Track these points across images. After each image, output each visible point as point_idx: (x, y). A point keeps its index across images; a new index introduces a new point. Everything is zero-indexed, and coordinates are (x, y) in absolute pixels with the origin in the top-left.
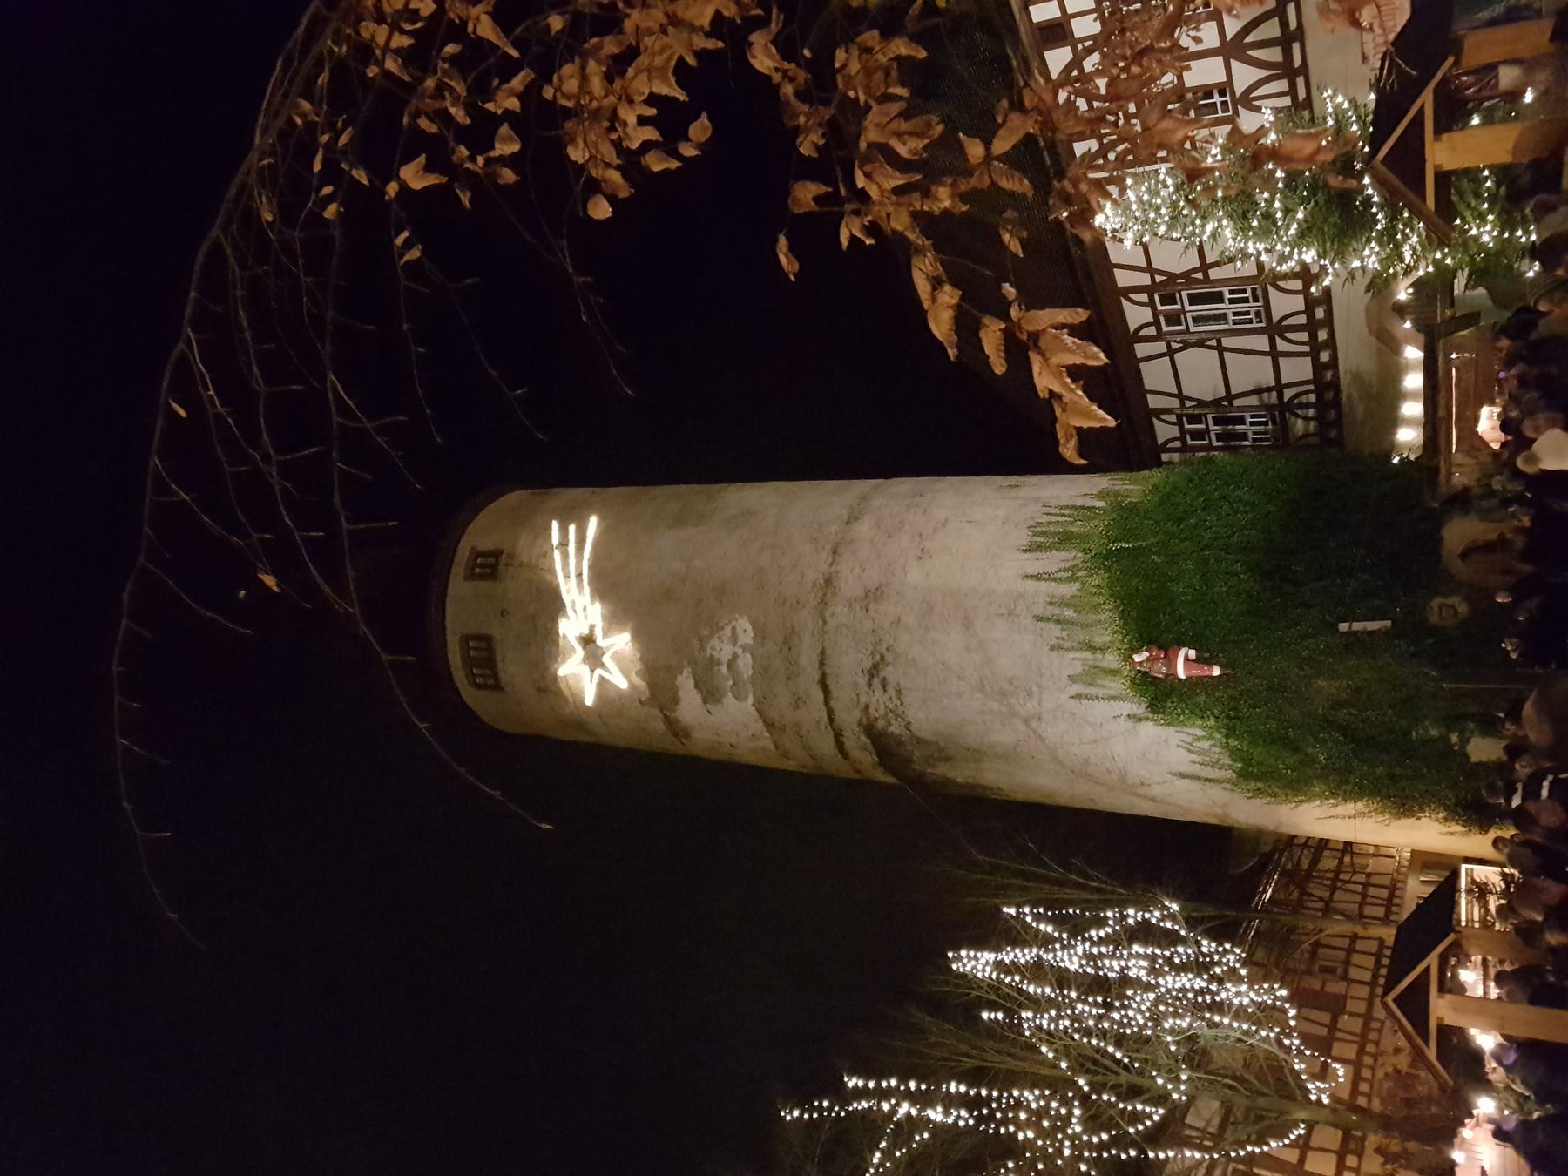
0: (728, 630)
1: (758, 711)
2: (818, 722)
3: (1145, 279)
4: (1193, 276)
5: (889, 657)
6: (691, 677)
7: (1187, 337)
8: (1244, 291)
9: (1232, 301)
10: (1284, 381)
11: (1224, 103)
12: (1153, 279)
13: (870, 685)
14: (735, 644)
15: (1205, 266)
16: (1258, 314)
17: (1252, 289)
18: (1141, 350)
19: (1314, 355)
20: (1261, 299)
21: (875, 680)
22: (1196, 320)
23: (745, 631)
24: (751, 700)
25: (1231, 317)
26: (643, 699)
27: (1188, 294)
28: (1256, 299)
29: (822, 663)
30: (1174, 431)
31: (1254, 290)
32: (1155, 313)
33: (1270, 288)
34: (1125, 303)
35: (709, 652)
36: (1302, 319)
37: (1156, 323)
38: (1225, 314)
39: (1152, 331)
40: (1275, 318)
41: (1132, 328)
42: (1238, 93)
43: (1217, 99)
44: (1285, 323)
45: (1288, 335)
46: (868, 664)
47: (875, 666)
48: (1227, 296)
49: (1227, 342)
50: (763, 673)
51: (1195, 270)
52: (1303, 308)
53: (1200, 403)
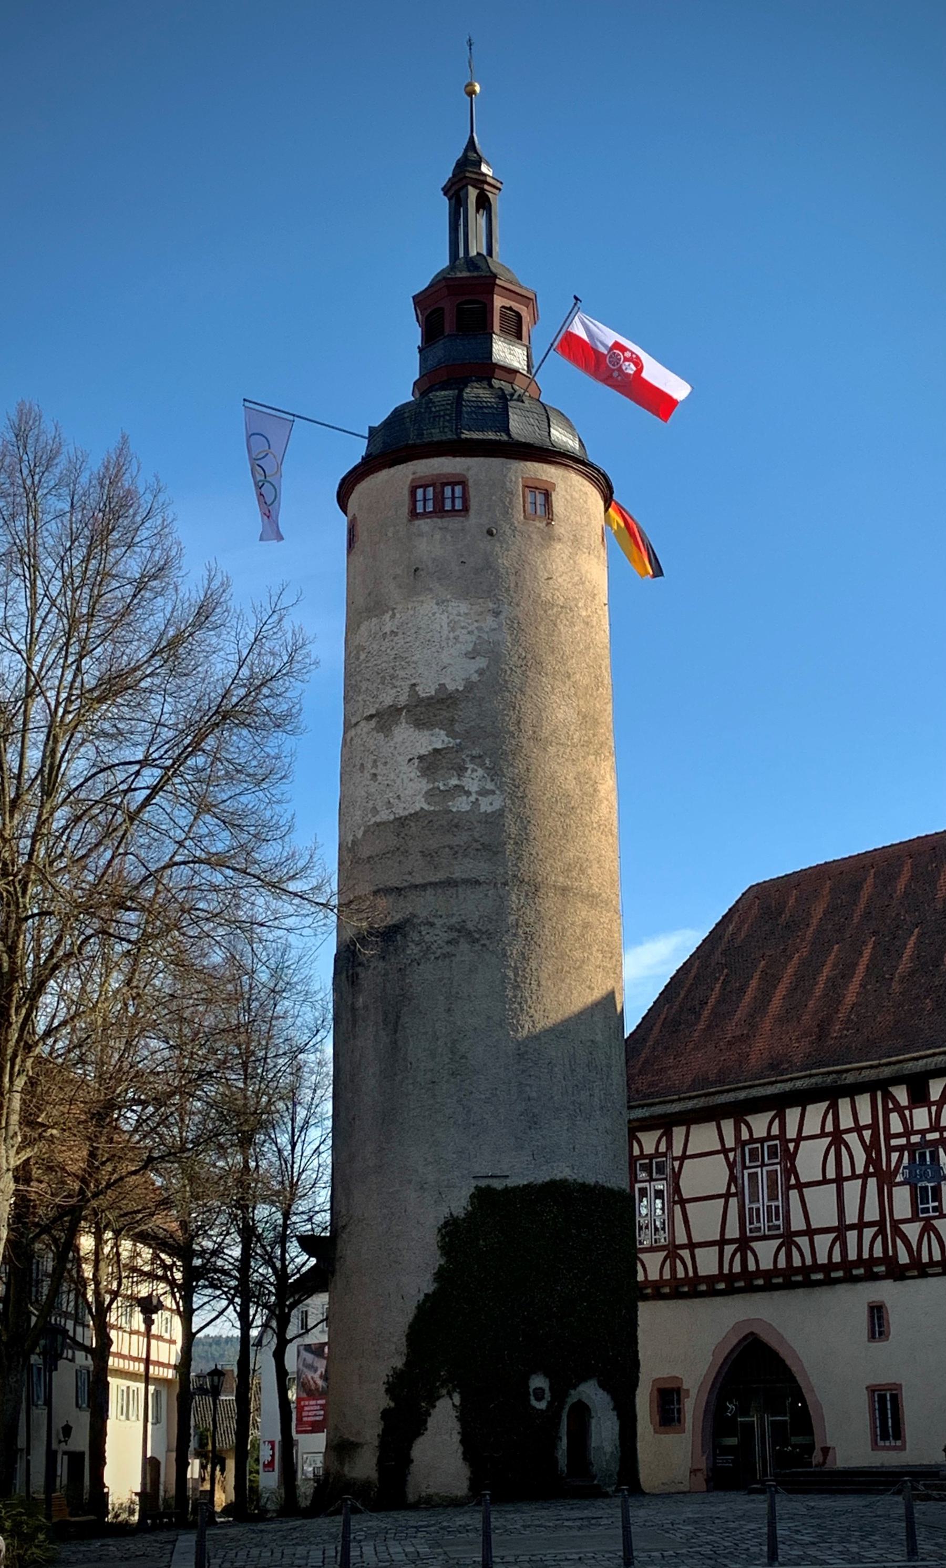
0: (490, 786)
1: (416, 813)
2: (410, 873)
3: (791, 1133)
4: (793, 1177)
5: (477, 947)
6: (444, 746)
7: (739, 1166)
8: (777, 1219)
9: (769, 1207)
10: (697, 1251)
11: (926, 1210)
12: (791, 1140)
13: (451, 928)
14: (476, 792)
15: (800, 1186)
16: (759, 1229)
17: (779, 1226)
18: (728, 1126)
19: (721, 1277)
20: (770, 1233)
21: (456, 934)
22: (753, 1176)
23: (491, 804)
24: (426, 807)
25: (755, 1206)
26: (417, 688)
27: (776, 1171)
28: (770, 1228)
29: (466, 882)
30: (649, 1149)
31: (778, 1227)
32: (762, 1141)
33: (781, 1240)
34: (773, 1113)
35: (470, 766)
36: (752, 1267)
37: (752, 1140)
38: (758, 1201)
39: (745, 1136)
40: (753, 1244)
41: (748, 1118)
42: (935, 1222)
43: (932, 1204)
44: (749, 1252)
45: (738, 1255)
46: (470, 926)
47: (470, 933)
48: (773, 1204)
49: (733, 1202)
50: (455, 824)
51: (797, 1178)
52: (762, 1267)
53: (677, 1176)
